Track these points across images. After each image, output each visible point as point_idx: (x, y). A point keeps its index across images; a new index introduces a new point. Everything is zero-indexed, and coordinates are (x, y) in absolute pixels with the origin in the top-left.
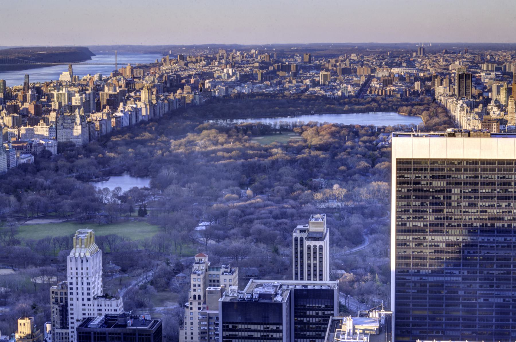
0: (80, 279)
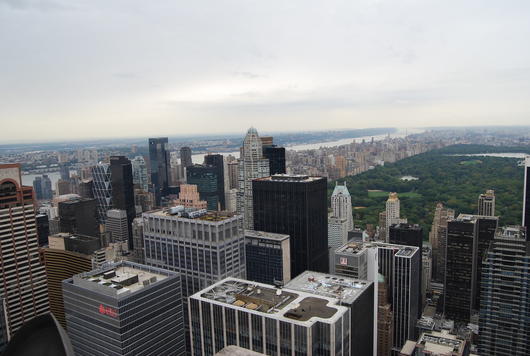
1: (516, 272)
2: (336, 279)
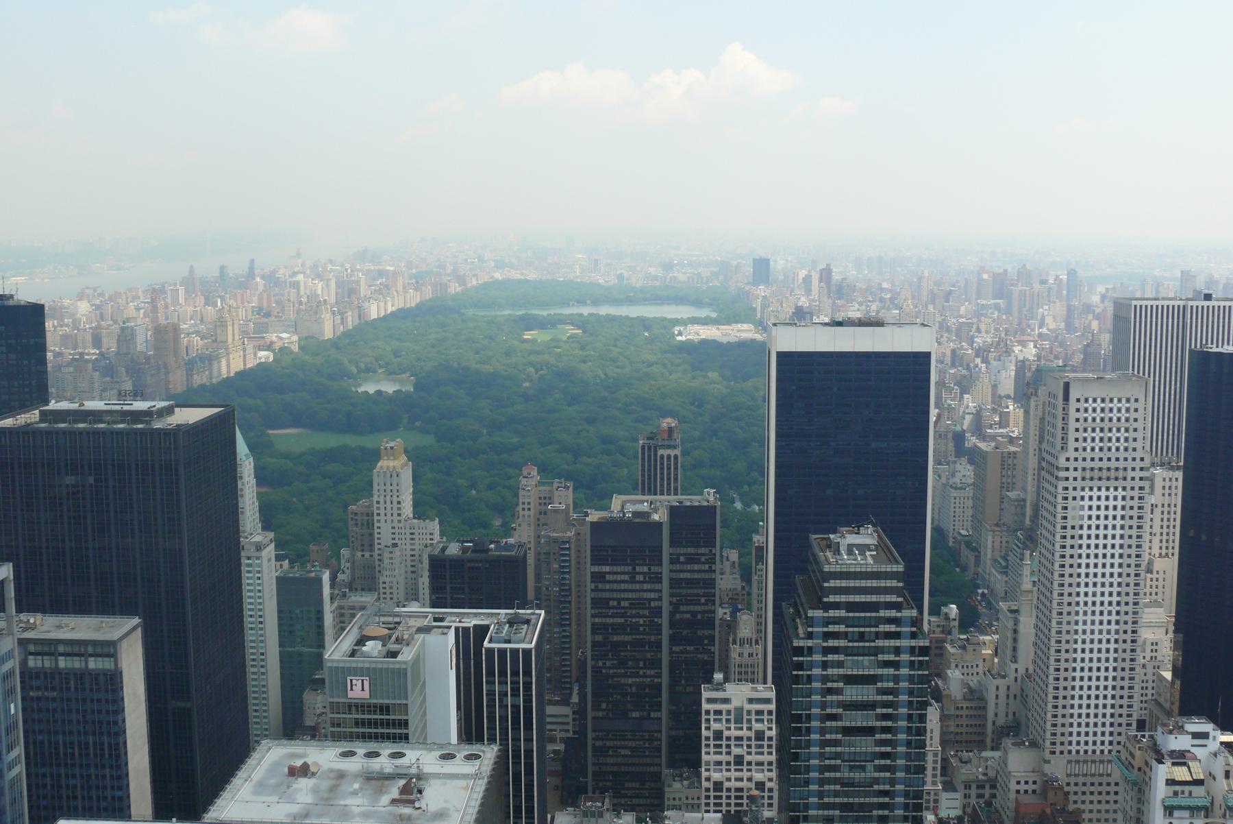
0: (388, 498)
1: (881, 657)
2: (377, 755)
